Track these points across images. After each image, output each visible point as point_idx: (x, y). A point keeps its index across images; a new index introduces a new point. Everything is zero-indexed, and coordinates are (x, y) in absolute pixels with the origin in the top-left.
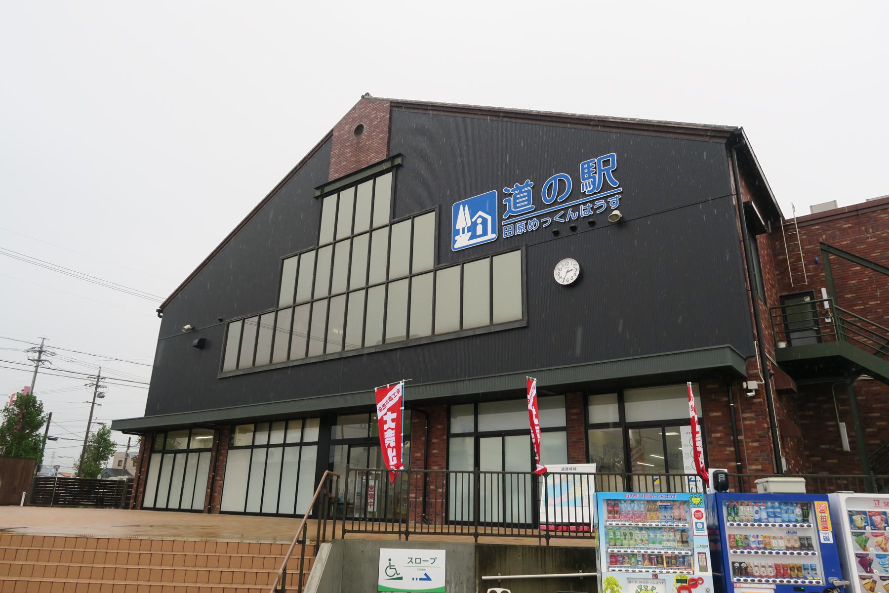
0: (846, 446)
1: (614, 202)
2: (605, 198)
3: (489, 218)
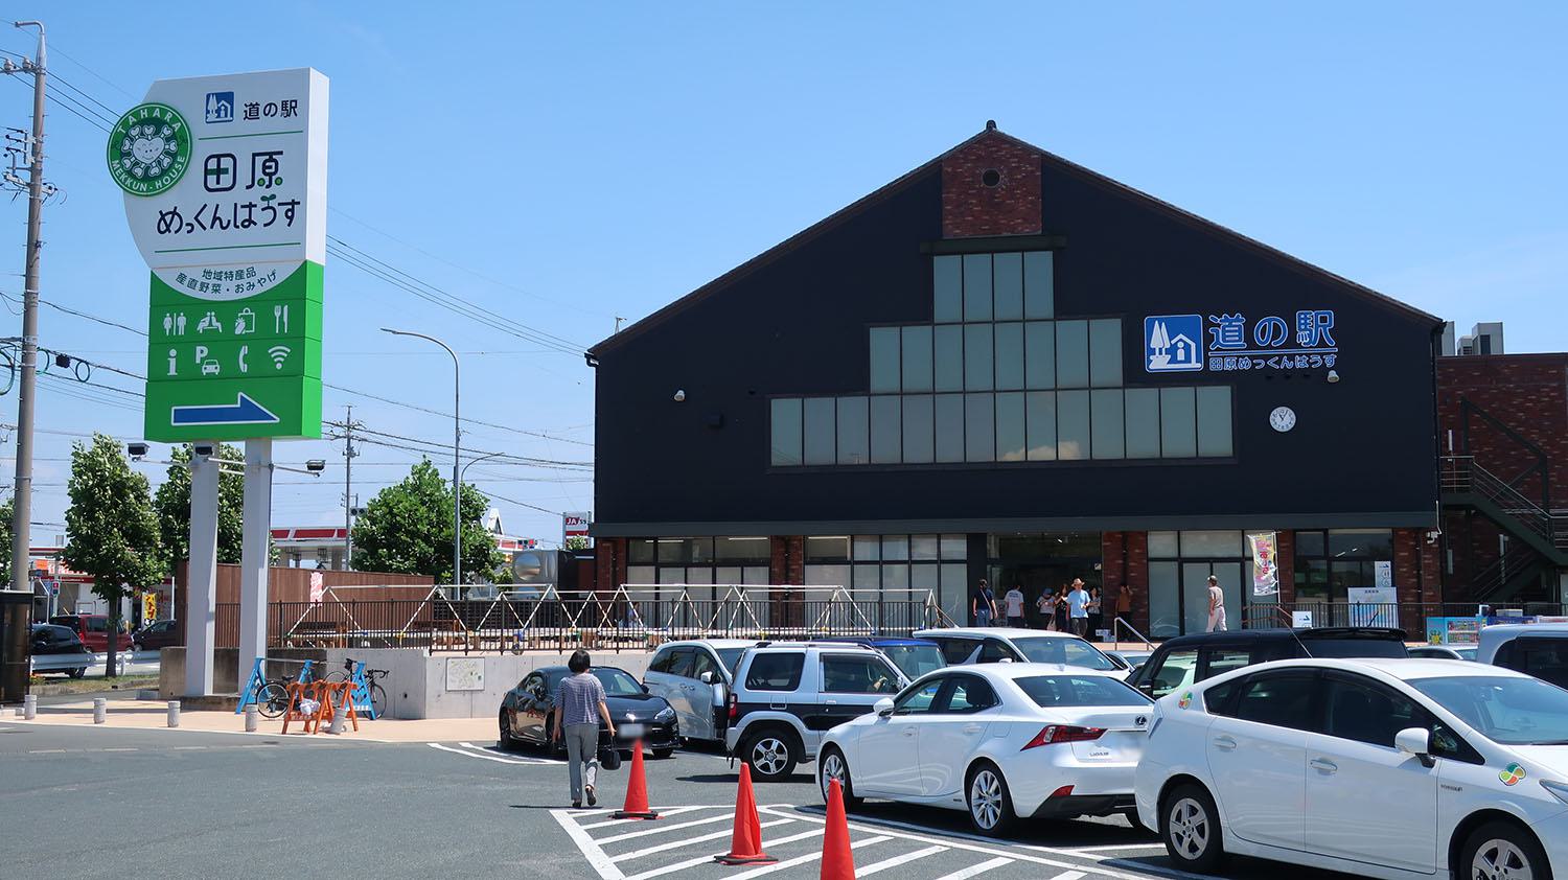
1: (1330, 361)
2: (1322, 355)
3: (1193, 345)
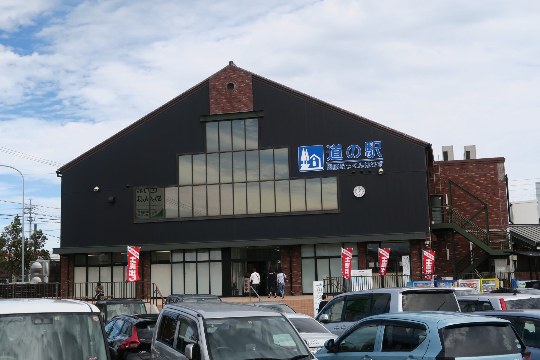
0: (448, 259)
1: (380, 164)
2: (376, 161)
3: (319, 159)
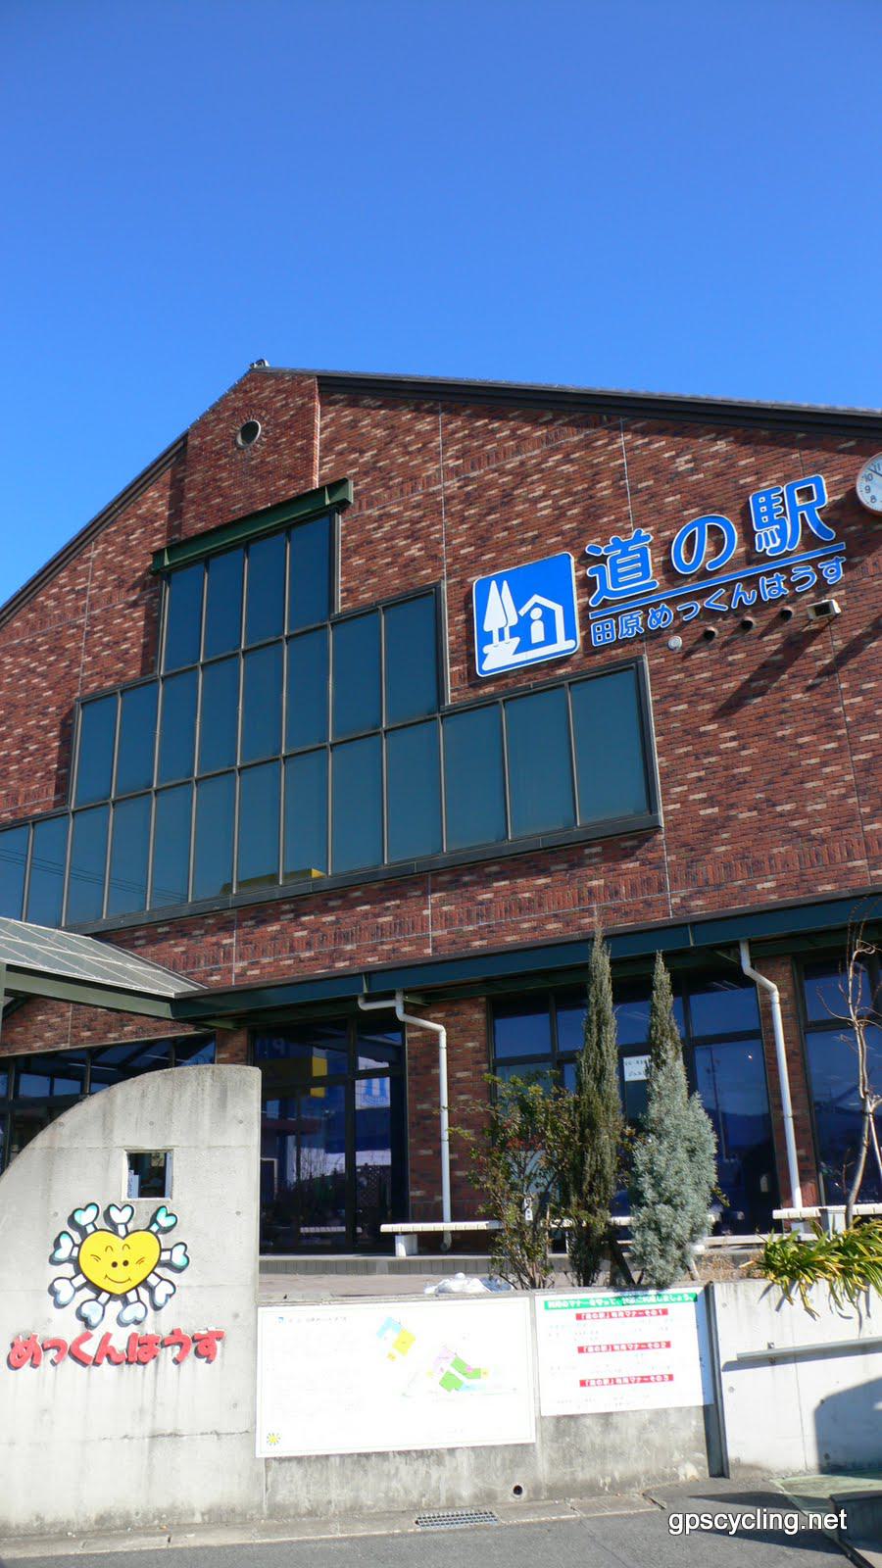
3: (558, 610)
